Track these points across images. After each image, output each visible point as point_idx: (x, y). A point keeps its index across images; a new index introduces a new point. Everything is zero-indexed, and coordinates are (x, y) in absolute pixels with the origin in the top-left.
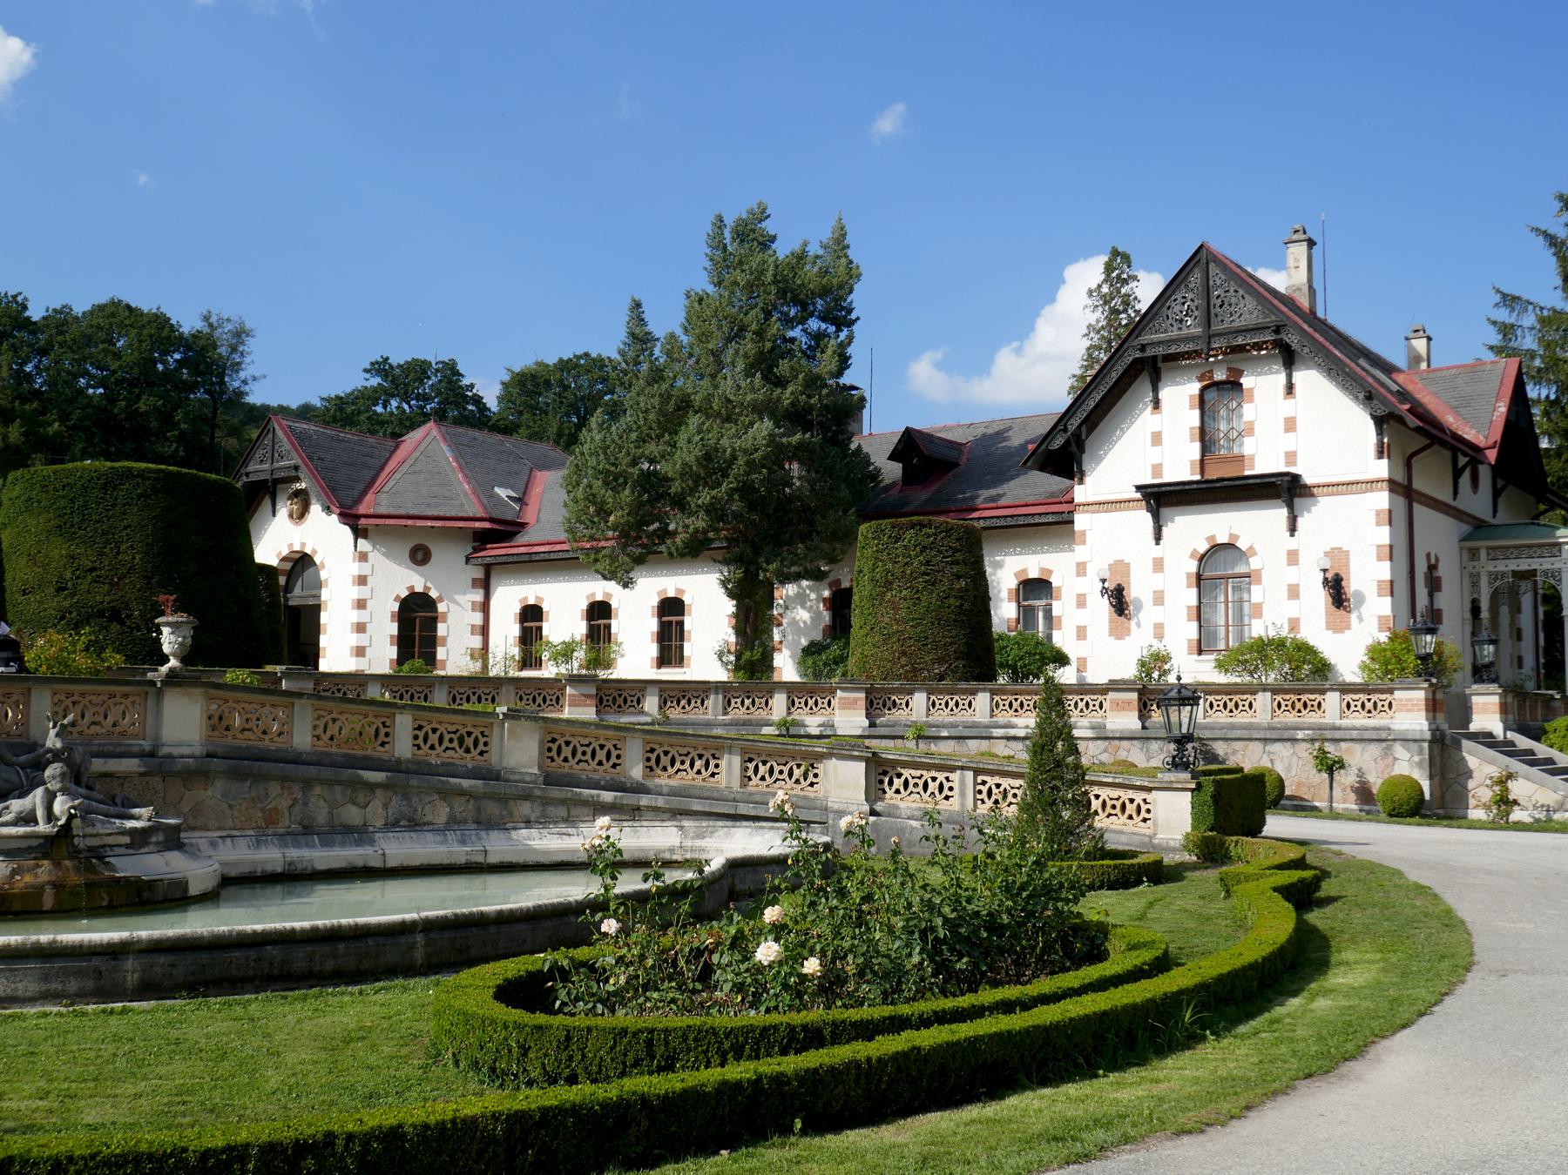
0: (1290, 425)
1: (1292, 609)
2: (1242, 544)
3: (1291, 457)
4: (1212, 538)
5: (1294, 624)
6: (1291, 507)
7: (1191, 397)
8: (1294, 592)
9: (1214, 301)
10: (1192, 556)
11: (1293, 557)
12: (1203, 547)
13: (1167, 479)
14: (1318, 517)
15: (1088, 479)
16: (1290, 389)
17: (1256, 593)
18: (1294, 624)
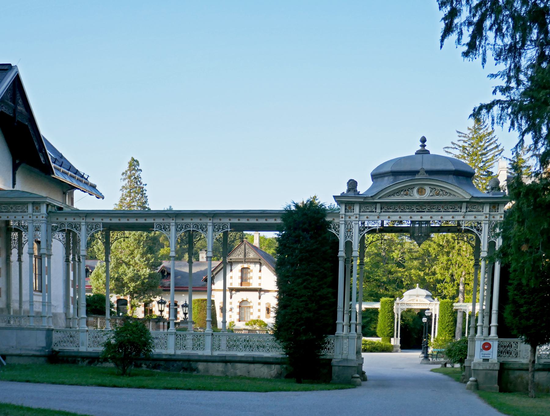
0: (260, 278)
1: (259, 314)
2: (249, 301)
3: (260, 284)
4: (243, 299)
5: (259, 317)
6: (259, 294)
7: (239, 270)
8: (259, 311)
9: (246, 252)
10: (238, 302)
11: (259, 304)
12: (241, 301)
13: (233, 287)
14: (264, 296)
15: (215, 285)
16: (260, 271)
17: (251, 310)
18: (259, 317)
